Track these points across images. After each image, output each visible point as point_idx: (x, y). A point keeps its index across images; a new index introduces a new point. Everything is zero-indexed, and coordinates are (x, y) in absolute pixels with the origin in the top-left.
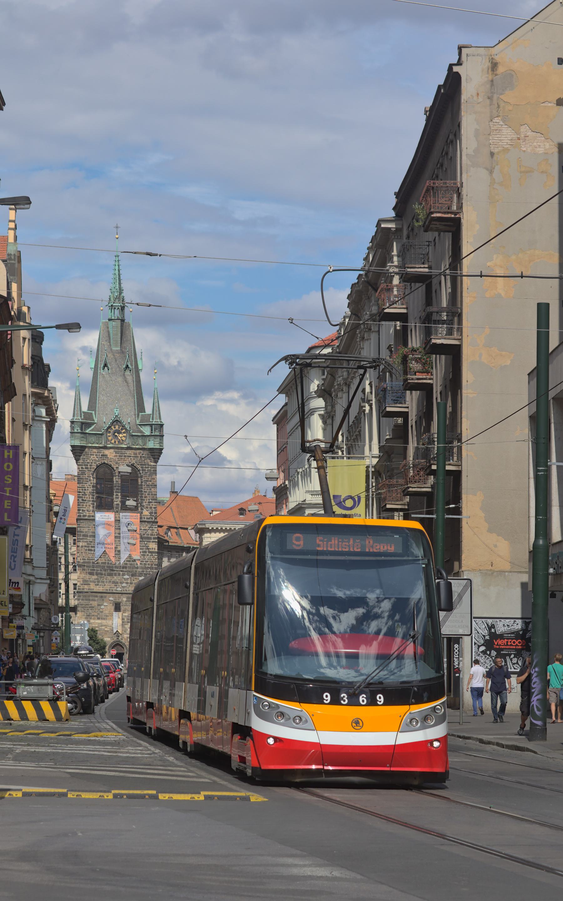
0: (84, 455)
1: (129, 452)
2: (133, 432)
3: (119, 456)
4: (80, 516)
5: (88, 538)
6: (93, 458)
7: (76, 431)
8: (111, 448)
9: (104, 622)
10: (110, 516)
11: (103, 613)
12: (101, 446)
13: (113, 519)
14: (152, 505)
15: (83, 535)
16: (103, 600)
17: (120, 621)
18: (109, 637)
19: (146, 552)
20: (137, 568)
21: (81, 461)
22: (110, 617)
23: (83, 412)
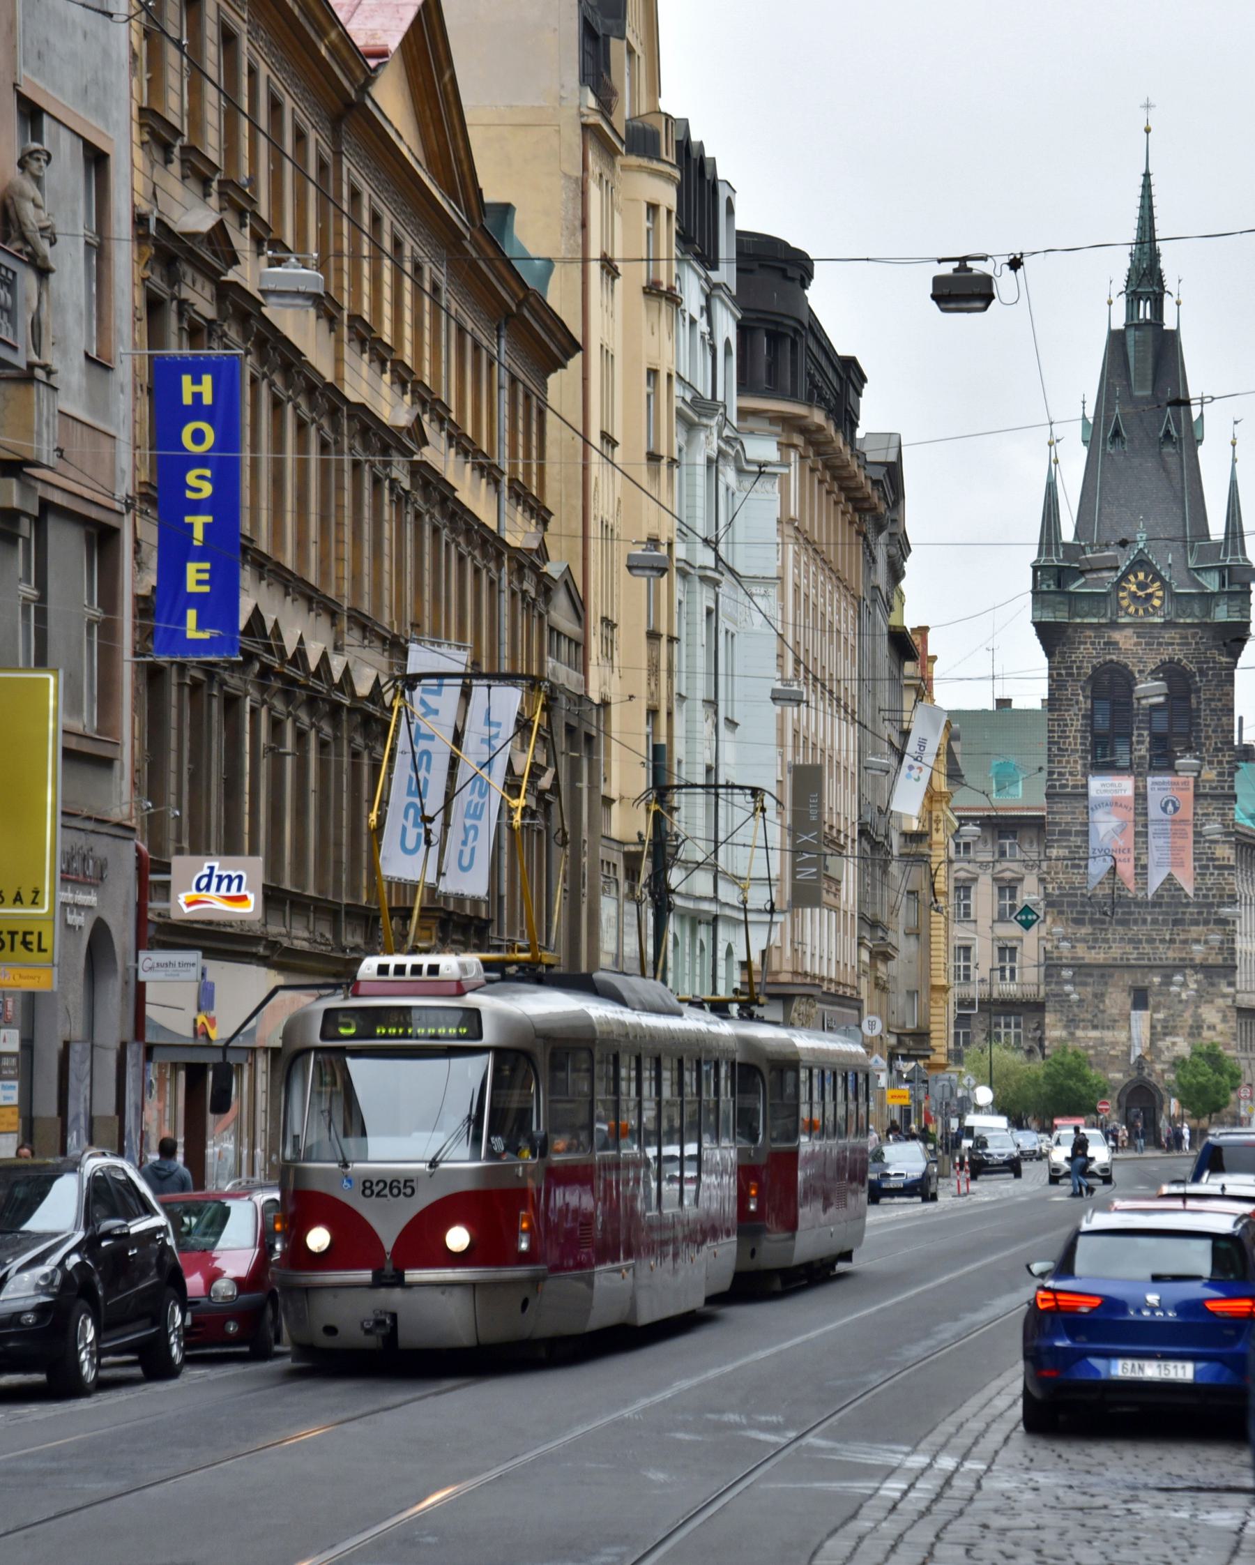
0: (1064, 645)
1: (1168, 635)
2: (1178, 587)
3: (1147, 644)
4: (1053, 787)
5: (1072, 838)
6: (1087, 655)
7: (1045, 588)
8: (1126, 625)
9: (1108, 1035)
10: (1124, 786)
11: (1106, 1016)
12: (1103, 621)
13: (1130, 792)
14: (1224, 756)
15: (1062, 833)
16: (1106, 984)
17: (1147, 1033)
18: (1119, 1071)
19: (1207, 867)
20: (1187, 905)
21: (1057, 659)
22: (1121, 1023)
23: (1064, 544)
